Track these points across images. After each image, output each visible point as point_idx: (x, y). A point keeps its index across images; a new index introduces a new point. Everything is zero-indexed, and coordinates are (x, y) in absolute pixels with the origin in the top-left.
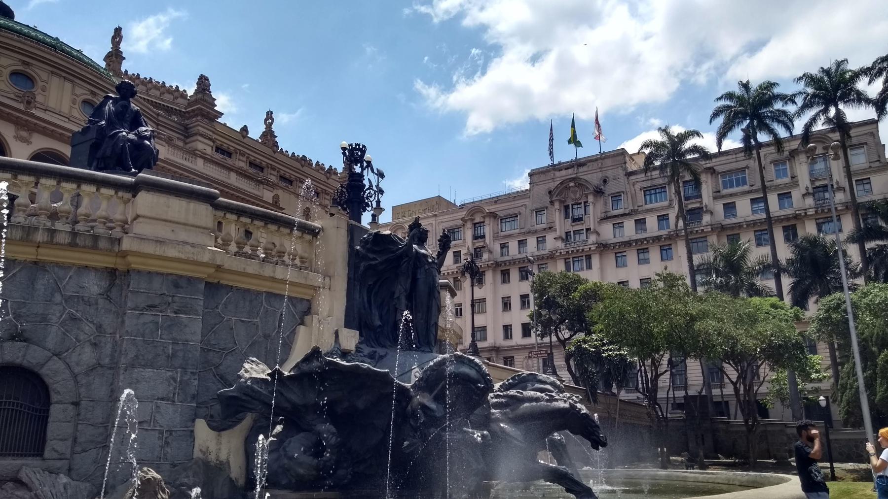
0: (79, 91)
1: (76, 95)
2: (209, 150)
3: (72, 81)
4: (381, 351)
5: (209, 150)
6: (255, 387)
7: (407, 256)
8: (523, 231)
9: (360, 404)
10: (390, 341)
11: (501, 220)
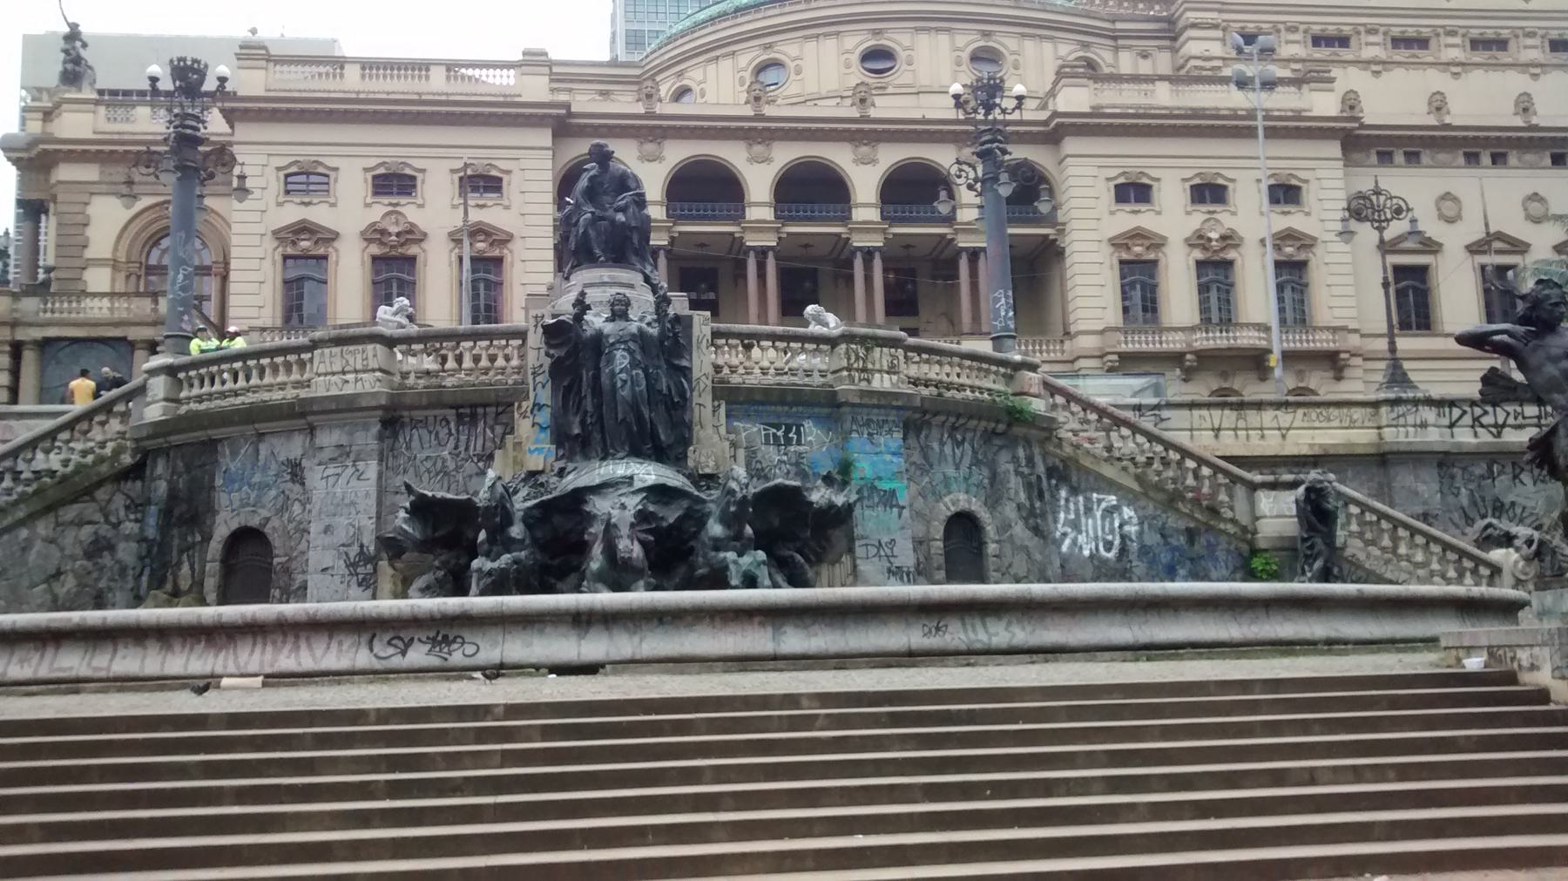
0: (961, 40)
1: (958, 49)
3: (948, 30)
6: (405, 527)
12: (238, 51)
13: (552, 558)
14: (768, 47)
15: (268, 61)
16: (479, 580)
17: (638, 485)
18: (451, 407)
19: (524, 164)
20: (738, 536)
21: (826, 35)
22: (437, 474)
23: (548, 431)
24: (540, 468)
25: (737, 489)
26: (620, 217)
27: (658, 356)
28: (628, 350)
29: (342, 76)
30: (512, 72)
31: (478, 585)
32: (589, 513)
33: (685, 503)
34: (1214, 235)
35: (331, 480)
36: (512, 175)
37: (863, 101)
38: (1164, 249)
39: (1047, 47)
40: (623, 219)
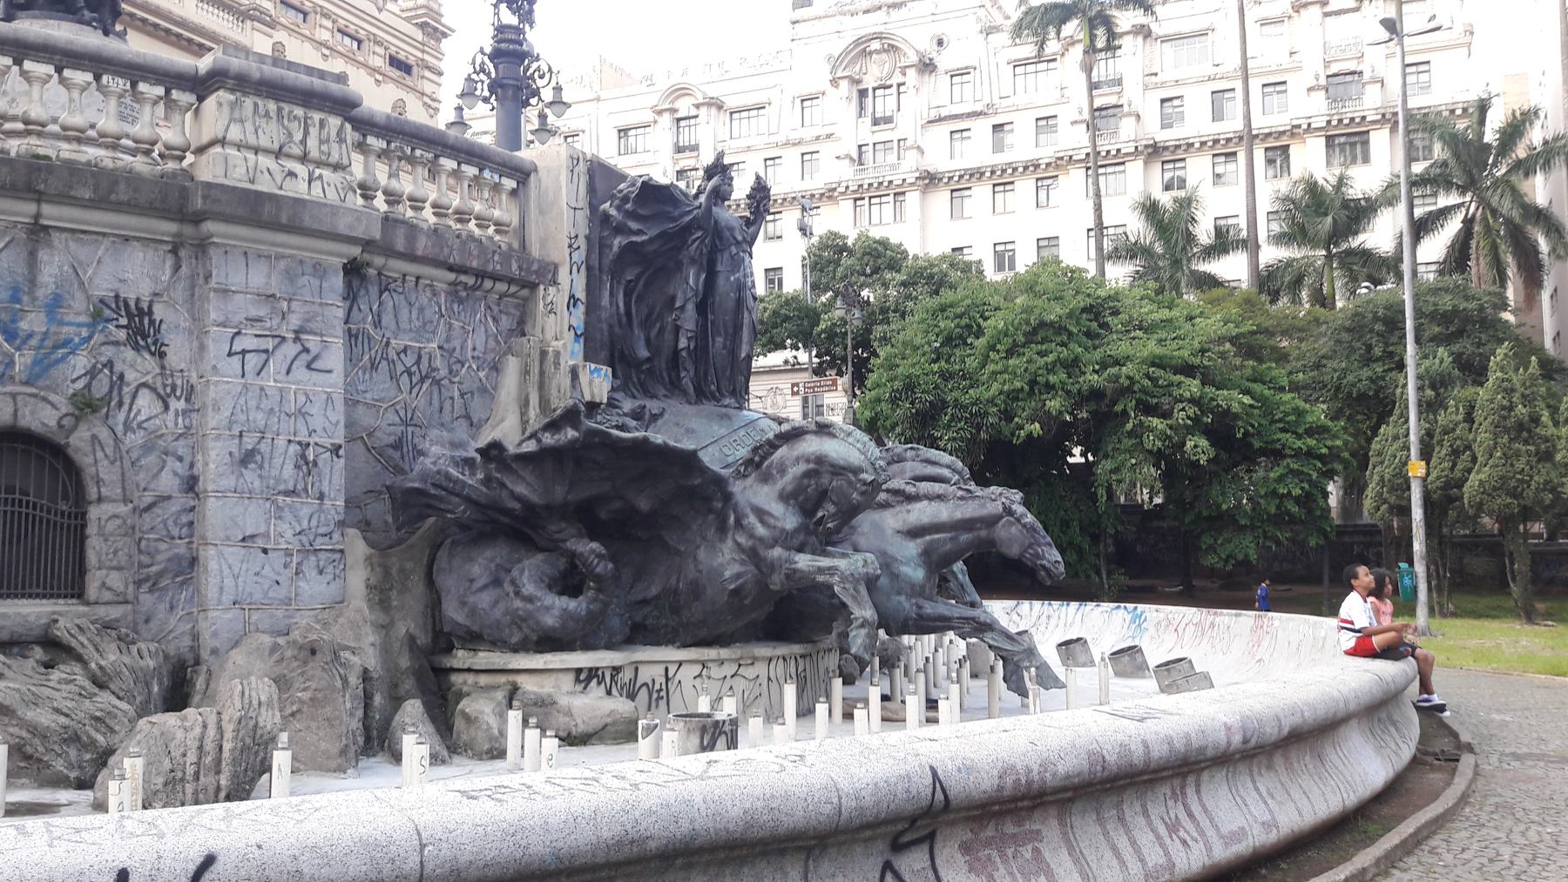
4: (653, 406)
6: (453, 472)
7: (700, 228)
8: (773, 139)
9: (644, 504)
10: (666, 389)
11: (731, 113)
18: (451, 269)
22: (422, 380)
23: (582, 340)
35: (253, 361)
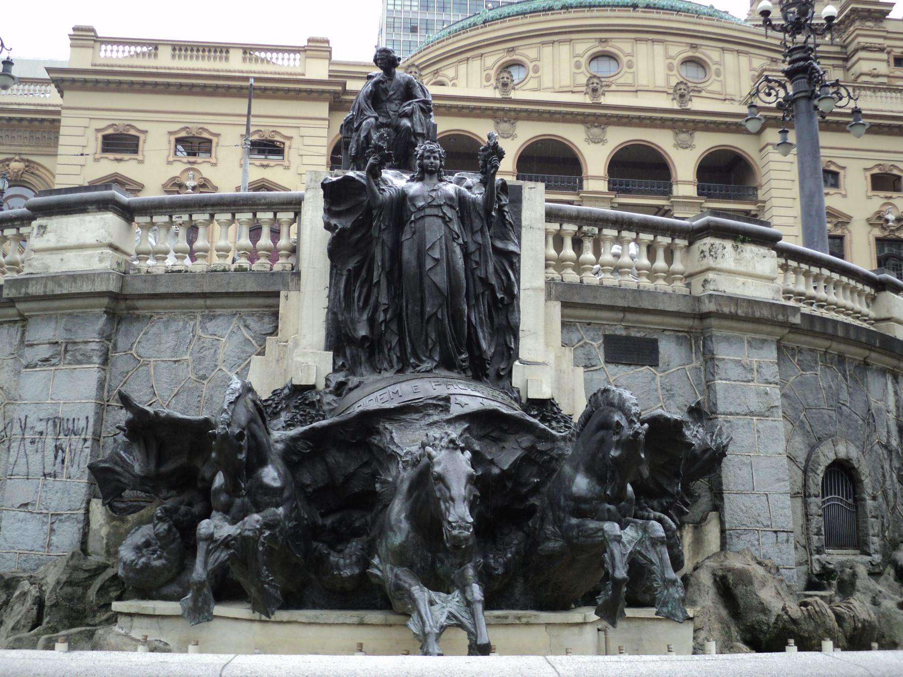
0: (674, 50)
1: (671, 58)
2: (882, 68)
5: (882, 68)
12: (72, 32)
13: (323, 516)
14: (511, 50)
15: (95, 41)
16: (208, 553)
17: (455, 410)
19: (304, 131)
20: (618, 497)
21: (560, 42)
24: (311, 383)
25: (624, 422)
26: (406, 122)
27: (482, 230)
28: (446, 221)
29: (156, 55)
30: (298, 56)
31: (206, 563)
32: (382, 450)
33: (526, 441)
34: (891, 217)
36: (293, 141)
37: (595, 90)
38: (849, 227)
39: (744, 60)
40: (409, 124)
